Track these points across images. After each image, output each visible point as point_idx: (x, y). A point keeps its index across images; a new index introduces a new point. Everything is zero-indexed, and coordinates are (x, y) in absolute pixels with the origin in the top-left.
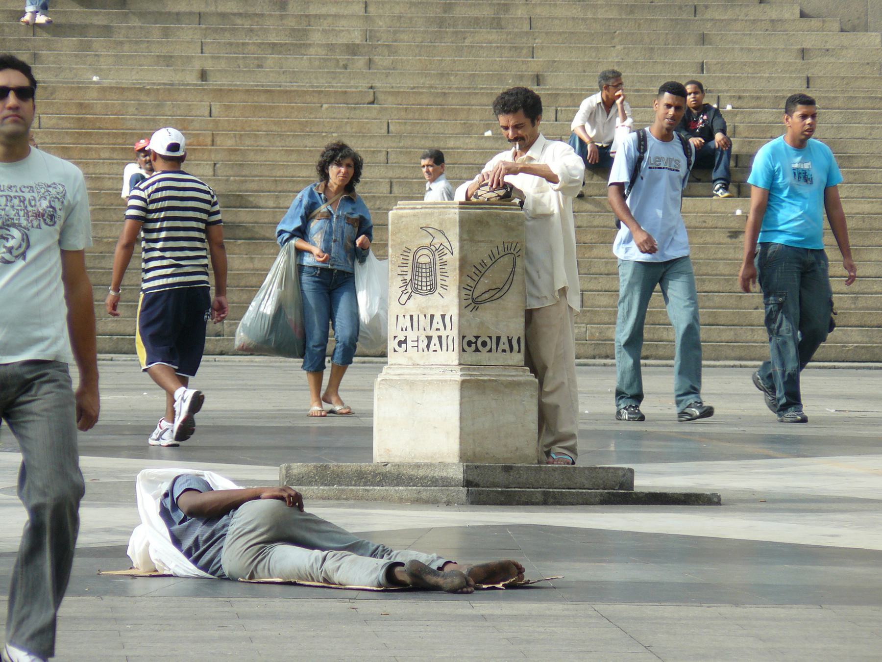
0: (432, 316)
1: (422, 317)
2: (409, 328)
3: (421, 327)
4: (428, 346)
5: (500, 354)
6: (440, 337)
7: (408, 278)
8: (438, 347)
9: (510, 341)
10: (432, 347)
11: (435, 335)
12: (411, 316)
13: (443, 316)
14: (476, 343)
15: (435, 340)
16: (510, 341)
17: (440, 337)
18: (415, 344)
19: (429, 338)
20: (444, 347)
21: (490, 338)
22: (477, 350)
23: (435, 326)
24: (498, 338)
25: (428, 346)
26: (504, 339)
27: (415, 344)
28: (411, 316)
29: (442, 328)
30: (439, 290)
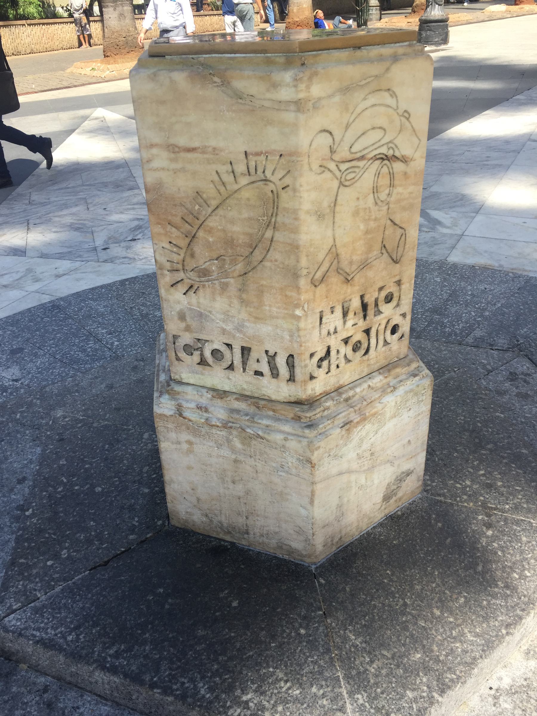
14: (201, 349)
16: (272, 359)
21: (229, 346)
24: (245, 351)
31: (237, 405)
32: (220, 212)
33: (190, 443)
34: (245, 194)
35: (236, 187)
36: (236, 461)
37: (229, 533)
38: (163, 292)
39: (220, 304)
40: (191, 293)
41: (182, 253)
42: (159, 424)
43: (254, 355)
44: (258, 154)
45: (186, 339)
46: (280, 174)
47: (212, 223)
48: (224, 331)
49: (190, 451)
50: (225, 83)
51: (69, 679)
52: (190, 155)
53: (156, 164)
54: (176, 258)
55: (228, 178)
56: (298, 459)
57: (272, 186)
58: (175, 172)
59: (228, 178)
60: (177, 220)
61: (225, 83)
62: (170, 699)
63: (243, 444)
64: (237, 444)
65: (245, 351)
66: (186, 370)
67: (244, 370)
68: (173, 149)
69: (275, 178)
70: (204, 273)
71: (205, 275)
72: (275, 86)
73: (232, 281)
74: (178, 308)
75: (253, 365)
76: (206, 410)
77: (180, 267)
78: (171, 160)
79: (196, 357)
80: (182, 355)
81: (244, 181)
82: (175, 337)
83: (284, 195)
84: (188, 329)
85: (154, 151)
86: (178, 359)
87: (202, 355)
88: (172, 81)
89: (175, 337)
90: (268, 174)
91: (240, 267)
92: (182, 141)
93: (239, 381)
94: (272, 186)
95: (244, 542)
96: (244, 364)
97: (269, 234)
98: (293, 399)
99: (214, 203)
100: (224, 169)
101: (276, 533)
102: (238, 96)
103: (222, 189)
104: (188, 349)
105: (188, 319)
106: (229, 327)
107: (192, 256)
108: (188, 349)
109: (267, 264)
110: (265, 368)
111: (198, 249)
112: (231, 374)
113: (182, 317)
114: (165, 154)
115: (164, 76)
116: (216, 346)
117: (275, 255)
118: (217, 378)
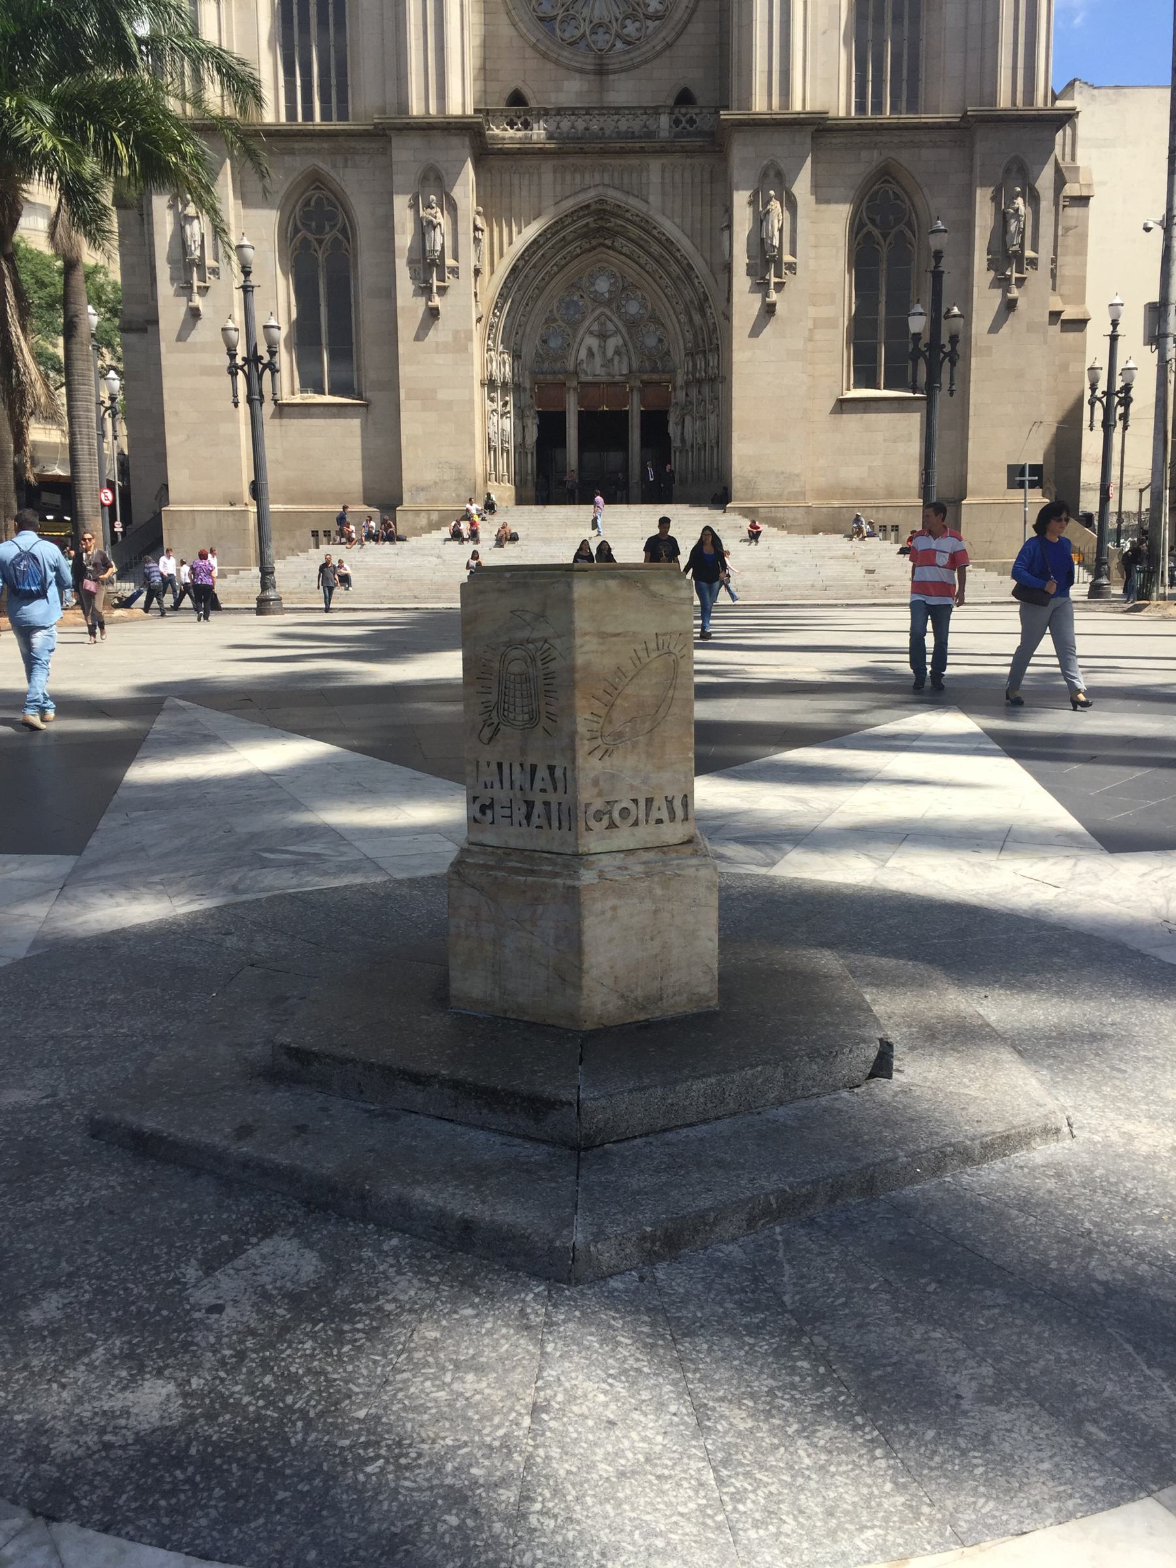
0: (534, 768)
1: (517, 769)
2: (497, 785)
3: (517, 784)
4: (528, 817)
5: (652, 827)
6: (547, 804)
7: (493, 698)
8: (542, 821)
9: (670, 802)
10: (535, 821)
11: (538, 799)
12: (500, 765)
13: (551, 769)
14: (610, 813)
15: (538, 809)
16: (670, 802)
17: (547, 804)
18: (507, 812)
19: (530, 805)
20: (555, 824)
21: (635, 801)
22: (612, 825)
23: (538, 784)
24: (649, 801)
25: (528, 817)
26: (659, 802)
27: (507, 812)
28: (500, 765)
29: (550, 788)
30: (544, 721)
31: (650, 856)
32: (635, 681)
33: (614, 908)
34: (655, 665)
35: (648, 660)
36: (655, 912)
37: (644, 1008)
38: (580, 761)
39: (631, 761)
40: (606, 757)
41: (601, 721)
42: (585, 897)
43: (656, 804)
44: (665, 634)
45: (598, 804)
46: (679, 647)
47: (630, 690)
48: (632, 787)
49: (614, 918)
50: (645, 587)
51: (661, 1122)
52: (614, 639)
53: (585, 649)
54: (595, 726)
55: (642, 654)
56: (708, 887)
57: (673, 657)
58: (602, 653)
59: (642, 654)
60: (600, 693)
61: (645, 587)
62: (759, 1069)
63: (663, 888)
64: (659, 892)
65: (649, 801)
66: (593, 842)
67: (647, 821)
68: (603, 635)
69: (676, 651)
70: (619, 736)
71: (620, 737)
72: (678, 589)
73: (641, 738)
74: (592, 775)
75: (655, 815)
76: (626, 869)
77: (599, 734)
78: (601, 644)
79: (605, 821)
80: (592, 823)
81: (654, 655)
82: (587, 805)
83: (682, 663)
84: (600, 794)
85: (587, 638)
86: (588, 829)
87: (611, 817)
88: (607, 586)
89: (587, 805)
90: (671, 648)
91: (648, 725)
92: (610, 629)
93: (645, 834)
94: (673, 657)
95: (658, 1014)
96: (647, 815)
97: (671, 693)
98: (686, 839)
99: (631, 675)
100: (640, 647)
101: (687, 984)
102: (654, 595)
103: (637, 662)
104: (598, 816)
105: (601, 783)
106: (637, 782)
107: (610, 722)
108: (598, 816)
109: (669, 718)
110: (664, 814)
111: (615, 715)
112: (636, 830)
113: (596, 782)
114: (595, 640)
115: (601, 584)
116: (624, 805)
117: (675, 710)
118: (625, 838)
